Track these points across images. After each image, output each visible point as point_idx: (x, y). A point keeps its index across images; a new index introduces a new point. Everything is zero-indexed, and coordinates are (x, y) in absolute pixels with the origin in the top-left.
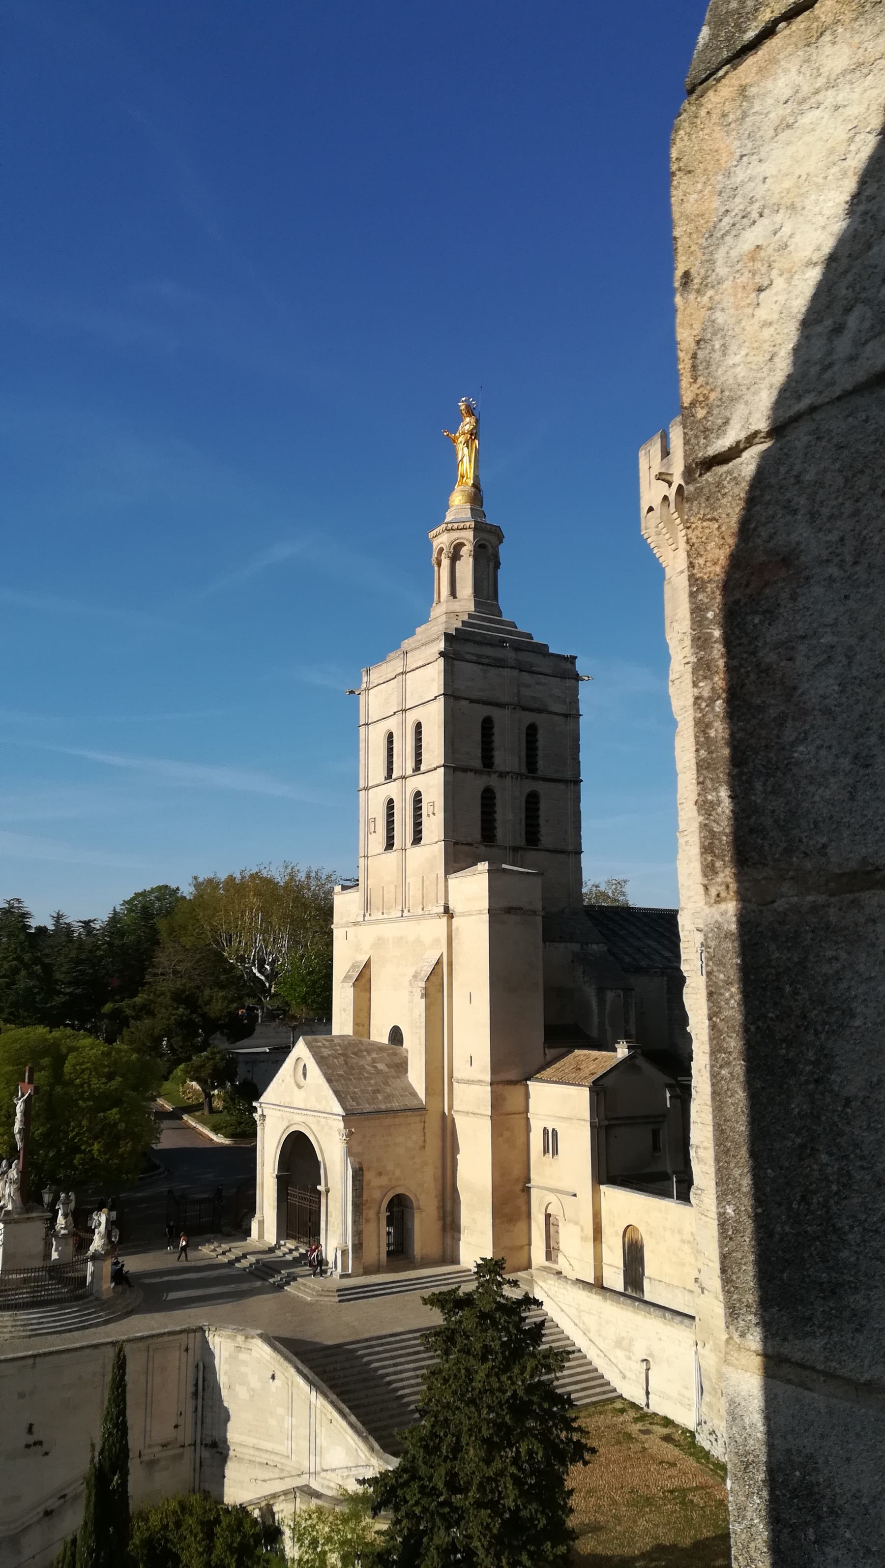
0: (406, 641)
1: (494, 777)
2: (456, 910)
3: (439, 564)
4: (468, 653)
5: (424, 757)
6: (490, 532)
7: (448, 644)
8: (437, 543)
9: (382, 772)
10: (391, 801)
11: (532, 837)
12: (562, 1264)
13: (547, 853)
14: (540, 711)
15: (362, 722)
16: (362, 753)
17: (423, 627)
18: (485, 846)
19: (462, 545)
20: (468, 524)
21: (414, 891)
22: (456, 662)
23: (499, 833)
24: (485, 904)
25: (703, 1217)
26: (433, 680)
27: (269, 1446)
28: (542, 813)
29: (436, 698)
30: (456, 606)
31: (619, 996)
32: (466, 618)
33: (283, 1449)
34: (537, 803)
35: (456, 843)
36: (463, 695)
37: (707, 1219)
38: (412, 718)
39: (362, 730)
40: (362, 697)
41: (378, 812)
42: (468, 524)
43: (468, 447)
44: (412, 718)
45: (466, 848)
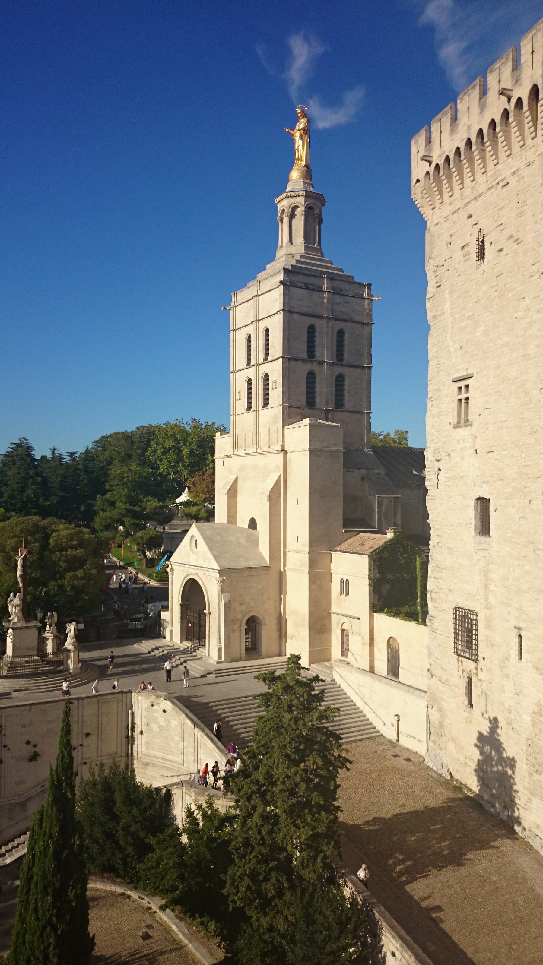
0: (260, 274)
1: (315, 364)
3: (282, 221)
4: (299, 282)
5: (270, 351)
6: (316, 198)
7: (286, 276)
8: (280, 206)
9: (244, 362)
10: (250, 380)
11: (339, 403)
12: (350, 658)
13: (349, 414)
14: (345, 321)
15: (231, 328)
16: (232, 349)
17: (271, 264)
18: (309, 409)
19: (297, 207)
20: (301, 193)
21: (264, 437)
22: (291, 288)
23: (318, 400)
24: (307, 446)
25: (433, 633)
26: (276, 300)
27: (171, 758)
28: (346, 387)
29: (278, 312)
30: (293, 250)
31: (391, 501)
32: (298, 258)
33: (179, 759)
34: (343, 381)
35: (290, 407)
36: (295, 310)
37: (436, 635)
38: (263, 325)
39: (232, 333)
40: (232, 312)
41: (242, 387)
42: (301, 193)
43: (301, 139)
44: (263, 325)
45: (297, 410)
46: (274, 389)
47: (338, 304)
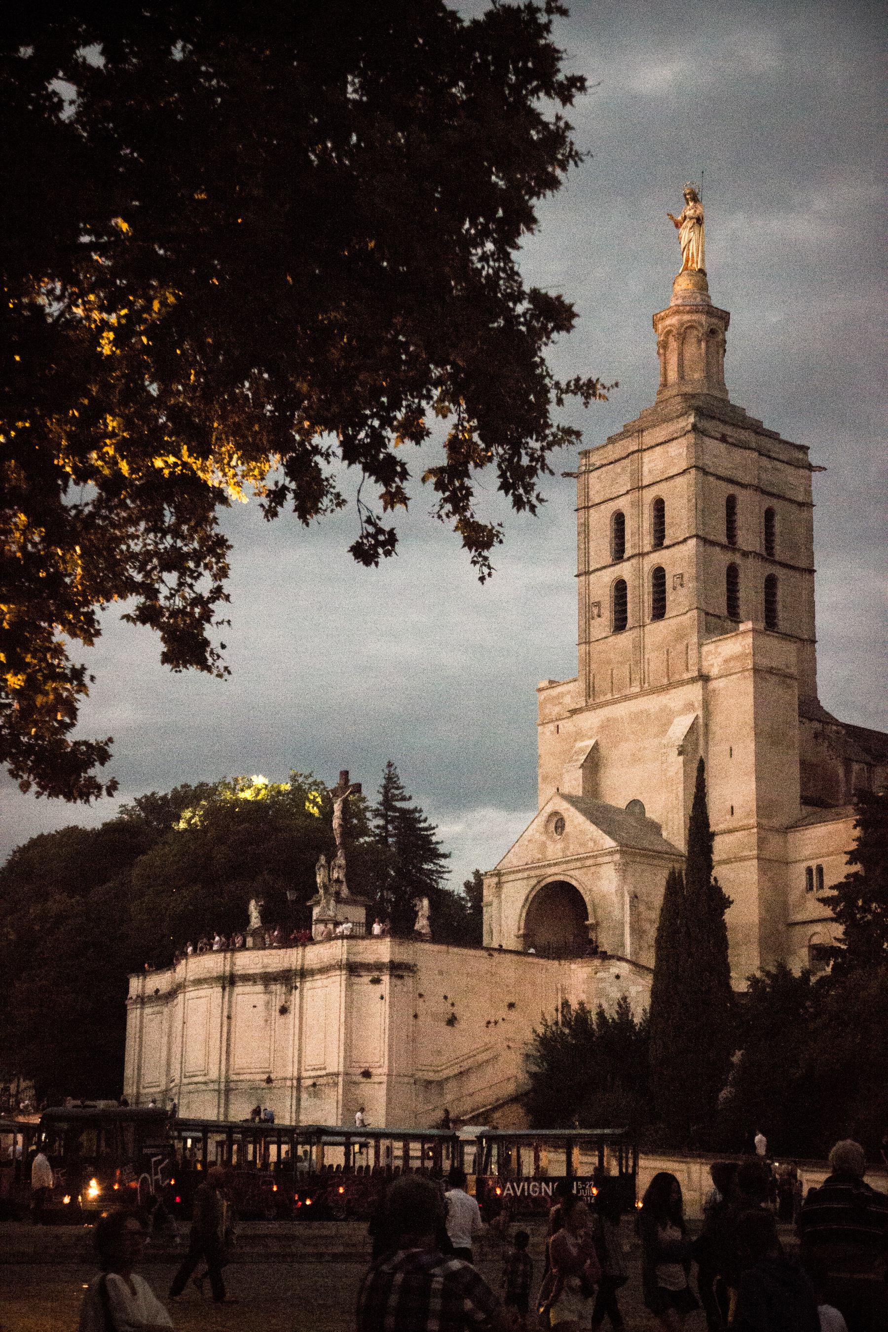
1: (738, 555)
2: (711, 674)
28: (779, 598)
44: (649, 496)
46: (679, 587)
47: (766, 470)
